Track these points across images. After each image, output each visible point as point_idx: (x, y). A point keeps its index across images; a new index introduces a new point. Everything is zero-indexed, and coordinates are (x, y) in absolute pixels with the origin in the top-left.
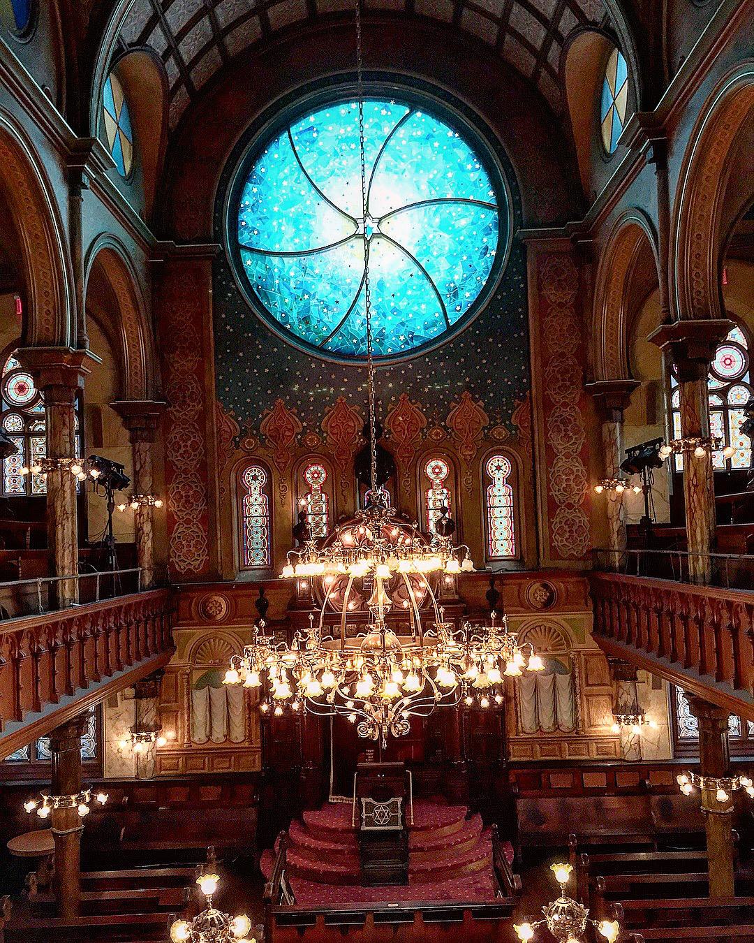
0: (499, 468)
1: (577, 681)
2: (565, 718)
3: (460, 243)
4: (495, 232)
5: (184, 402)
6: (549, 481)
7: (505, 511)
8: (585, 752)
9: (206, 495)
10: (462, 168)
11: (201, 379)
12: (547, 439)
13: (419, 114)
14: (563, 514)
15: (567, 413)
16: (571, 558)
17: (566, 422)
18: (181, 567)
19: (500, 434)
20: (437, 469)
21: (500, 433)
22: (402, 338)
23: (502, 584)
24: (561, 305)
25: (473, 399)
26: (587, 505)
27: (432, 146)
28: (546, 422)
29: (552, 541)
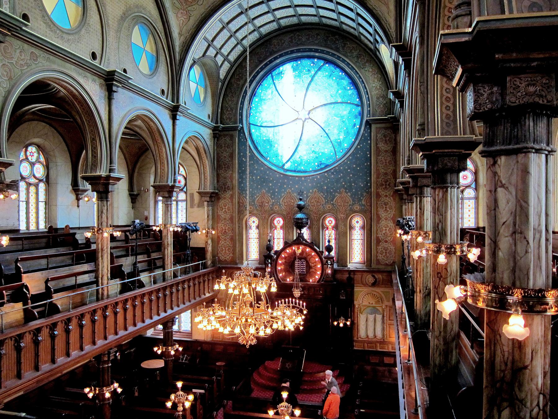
0: (357, 222)
1: (385, 318)
2: (379, 334)
3: (343, 122)
4: (359, 117)
5: (225, 190)
6: (377, 230)
7: (360, 242)
8: (386, 348)
9: (232, 229)
10: (345, 88)
11: (232, 182)
12: (377, 211)
13: (327, 65)
14: (383, 245)
15: (387, 200)
16: (387, 265)
17: (386, 204)
18: (222, 258)
19: (357, 208)
20: (330, 221)
21: (357, 207)
22: (316, 164)
23: (354, 274)
24: (386, 151)
25: (346, 192)
26: (394, 241)
27: (332, 79)
28: (377, 203)
29: (377, 257)
